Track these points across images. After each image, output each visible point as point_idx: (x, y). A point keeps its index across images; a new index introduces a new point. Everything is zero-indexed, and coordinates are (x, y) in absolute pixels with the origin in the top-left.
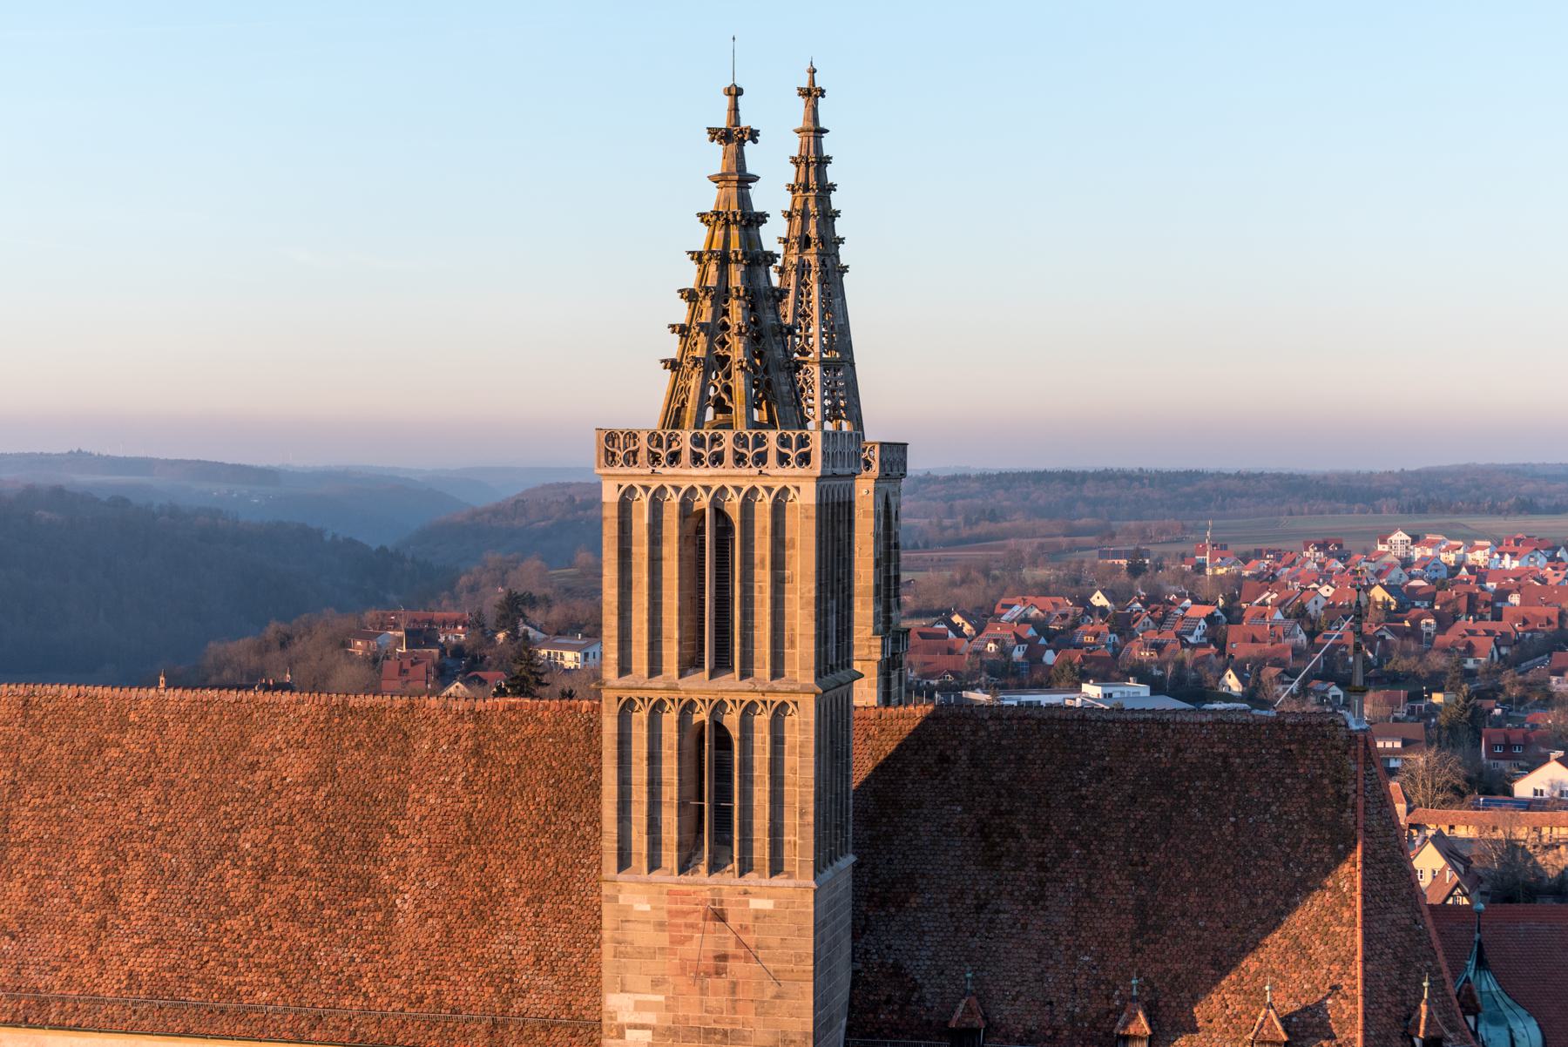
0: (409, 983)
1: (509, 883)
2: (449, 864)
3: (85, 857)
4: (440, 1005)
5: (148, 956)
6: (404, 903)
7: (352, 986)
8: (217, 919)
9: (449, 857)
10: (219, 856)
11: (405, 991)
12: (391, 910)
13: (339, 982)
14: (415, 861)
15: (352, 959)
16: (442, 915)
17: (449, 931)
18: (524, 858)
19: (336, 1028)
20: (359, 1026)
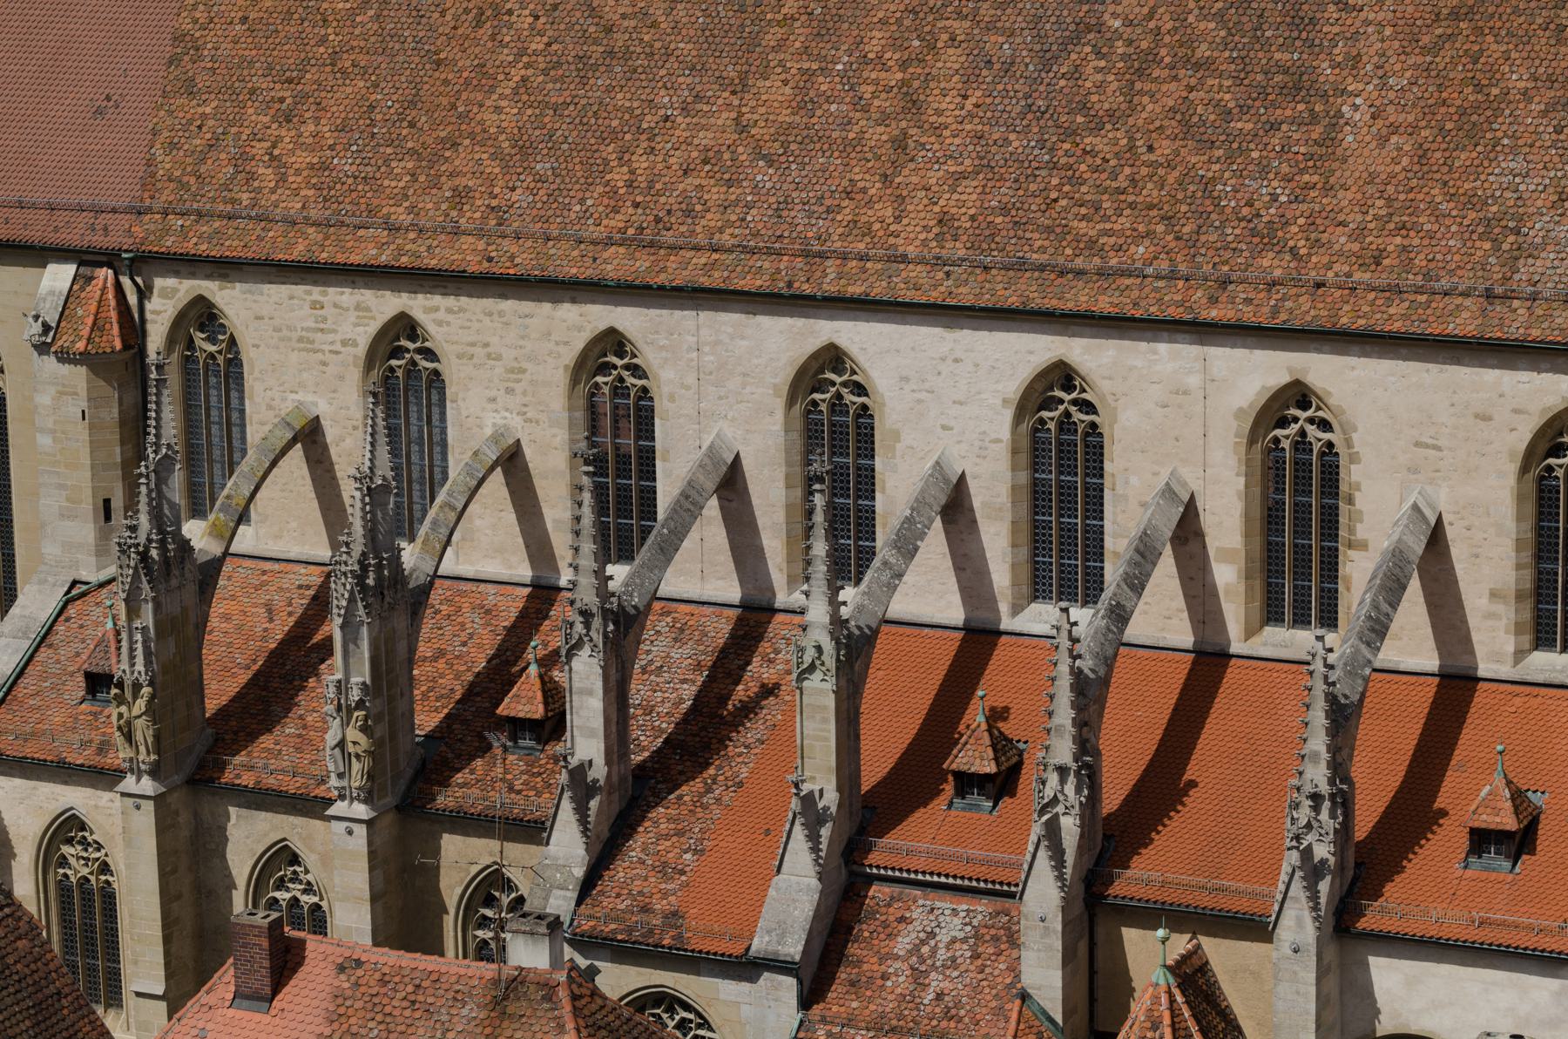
0: (1359, 233)
1: (1517, 80)
2: (1425, 50)
3: (875, 41)
4: (1408, 266)
5: (969, 192)
6: (1355, 111)
7: (1268, 238)
8: (1071, 133)
9: (1426, 40)
10: (1076, 39)
11: (1356, 247)
12: (1336, 122)
13: (1254, 233)
14: (1370, 48)
15: (1274, 198)
16: (1414, 129)
17: (1422, 156)
18: (1542, 41)
19: (1248, 301)
20: (1283, 299)
